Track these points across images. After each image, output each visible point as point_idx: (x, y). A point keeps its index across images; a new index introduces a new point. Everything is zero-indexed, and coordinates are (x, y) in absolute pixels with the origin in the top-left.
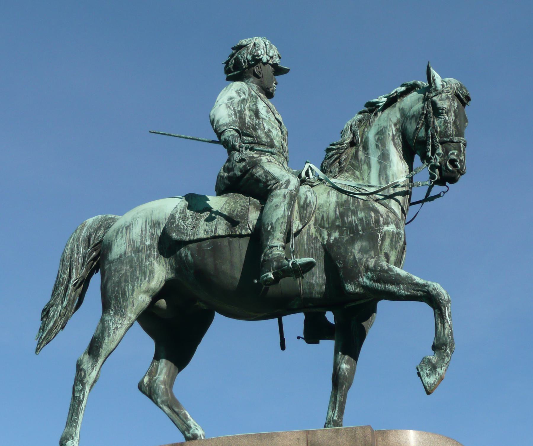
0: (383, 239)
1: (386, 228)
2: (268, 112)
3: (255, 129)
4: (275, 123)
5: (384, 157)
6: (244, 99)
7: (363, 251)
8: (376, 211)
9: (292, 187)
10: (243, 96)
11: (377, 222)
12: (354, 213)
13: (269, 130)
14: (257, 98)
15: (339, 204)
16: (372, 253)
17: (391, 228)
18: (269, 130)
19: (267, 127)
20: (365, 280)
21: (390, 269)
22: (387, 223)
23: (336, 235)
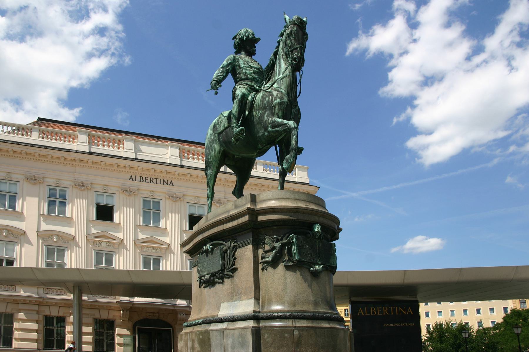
0: (275, 108)
1: (275, 102)
2: (244, 64)
3: (240, 74)
4: (248, 67)
5: (280, 67)
6: (230, 63)
7: (268, 116)
8: (272, 95)
9: (239, 97)
10: (230, 61)
11: (272, 100)
12: (265, 99)
13: (246, 72)
14: (238, 59)
15: (262, 97)
16: (271, 115)
17: (278, 100)
18: (246, 72)
19: (244, 71)
20: (270, 129)
21: (275, 121)
22: (275, 100)
23: (261, 112)
